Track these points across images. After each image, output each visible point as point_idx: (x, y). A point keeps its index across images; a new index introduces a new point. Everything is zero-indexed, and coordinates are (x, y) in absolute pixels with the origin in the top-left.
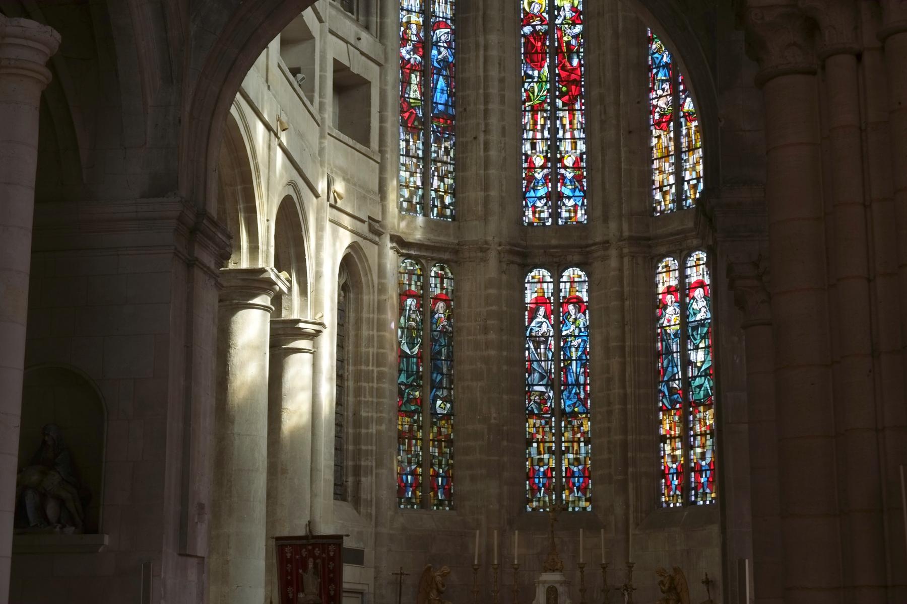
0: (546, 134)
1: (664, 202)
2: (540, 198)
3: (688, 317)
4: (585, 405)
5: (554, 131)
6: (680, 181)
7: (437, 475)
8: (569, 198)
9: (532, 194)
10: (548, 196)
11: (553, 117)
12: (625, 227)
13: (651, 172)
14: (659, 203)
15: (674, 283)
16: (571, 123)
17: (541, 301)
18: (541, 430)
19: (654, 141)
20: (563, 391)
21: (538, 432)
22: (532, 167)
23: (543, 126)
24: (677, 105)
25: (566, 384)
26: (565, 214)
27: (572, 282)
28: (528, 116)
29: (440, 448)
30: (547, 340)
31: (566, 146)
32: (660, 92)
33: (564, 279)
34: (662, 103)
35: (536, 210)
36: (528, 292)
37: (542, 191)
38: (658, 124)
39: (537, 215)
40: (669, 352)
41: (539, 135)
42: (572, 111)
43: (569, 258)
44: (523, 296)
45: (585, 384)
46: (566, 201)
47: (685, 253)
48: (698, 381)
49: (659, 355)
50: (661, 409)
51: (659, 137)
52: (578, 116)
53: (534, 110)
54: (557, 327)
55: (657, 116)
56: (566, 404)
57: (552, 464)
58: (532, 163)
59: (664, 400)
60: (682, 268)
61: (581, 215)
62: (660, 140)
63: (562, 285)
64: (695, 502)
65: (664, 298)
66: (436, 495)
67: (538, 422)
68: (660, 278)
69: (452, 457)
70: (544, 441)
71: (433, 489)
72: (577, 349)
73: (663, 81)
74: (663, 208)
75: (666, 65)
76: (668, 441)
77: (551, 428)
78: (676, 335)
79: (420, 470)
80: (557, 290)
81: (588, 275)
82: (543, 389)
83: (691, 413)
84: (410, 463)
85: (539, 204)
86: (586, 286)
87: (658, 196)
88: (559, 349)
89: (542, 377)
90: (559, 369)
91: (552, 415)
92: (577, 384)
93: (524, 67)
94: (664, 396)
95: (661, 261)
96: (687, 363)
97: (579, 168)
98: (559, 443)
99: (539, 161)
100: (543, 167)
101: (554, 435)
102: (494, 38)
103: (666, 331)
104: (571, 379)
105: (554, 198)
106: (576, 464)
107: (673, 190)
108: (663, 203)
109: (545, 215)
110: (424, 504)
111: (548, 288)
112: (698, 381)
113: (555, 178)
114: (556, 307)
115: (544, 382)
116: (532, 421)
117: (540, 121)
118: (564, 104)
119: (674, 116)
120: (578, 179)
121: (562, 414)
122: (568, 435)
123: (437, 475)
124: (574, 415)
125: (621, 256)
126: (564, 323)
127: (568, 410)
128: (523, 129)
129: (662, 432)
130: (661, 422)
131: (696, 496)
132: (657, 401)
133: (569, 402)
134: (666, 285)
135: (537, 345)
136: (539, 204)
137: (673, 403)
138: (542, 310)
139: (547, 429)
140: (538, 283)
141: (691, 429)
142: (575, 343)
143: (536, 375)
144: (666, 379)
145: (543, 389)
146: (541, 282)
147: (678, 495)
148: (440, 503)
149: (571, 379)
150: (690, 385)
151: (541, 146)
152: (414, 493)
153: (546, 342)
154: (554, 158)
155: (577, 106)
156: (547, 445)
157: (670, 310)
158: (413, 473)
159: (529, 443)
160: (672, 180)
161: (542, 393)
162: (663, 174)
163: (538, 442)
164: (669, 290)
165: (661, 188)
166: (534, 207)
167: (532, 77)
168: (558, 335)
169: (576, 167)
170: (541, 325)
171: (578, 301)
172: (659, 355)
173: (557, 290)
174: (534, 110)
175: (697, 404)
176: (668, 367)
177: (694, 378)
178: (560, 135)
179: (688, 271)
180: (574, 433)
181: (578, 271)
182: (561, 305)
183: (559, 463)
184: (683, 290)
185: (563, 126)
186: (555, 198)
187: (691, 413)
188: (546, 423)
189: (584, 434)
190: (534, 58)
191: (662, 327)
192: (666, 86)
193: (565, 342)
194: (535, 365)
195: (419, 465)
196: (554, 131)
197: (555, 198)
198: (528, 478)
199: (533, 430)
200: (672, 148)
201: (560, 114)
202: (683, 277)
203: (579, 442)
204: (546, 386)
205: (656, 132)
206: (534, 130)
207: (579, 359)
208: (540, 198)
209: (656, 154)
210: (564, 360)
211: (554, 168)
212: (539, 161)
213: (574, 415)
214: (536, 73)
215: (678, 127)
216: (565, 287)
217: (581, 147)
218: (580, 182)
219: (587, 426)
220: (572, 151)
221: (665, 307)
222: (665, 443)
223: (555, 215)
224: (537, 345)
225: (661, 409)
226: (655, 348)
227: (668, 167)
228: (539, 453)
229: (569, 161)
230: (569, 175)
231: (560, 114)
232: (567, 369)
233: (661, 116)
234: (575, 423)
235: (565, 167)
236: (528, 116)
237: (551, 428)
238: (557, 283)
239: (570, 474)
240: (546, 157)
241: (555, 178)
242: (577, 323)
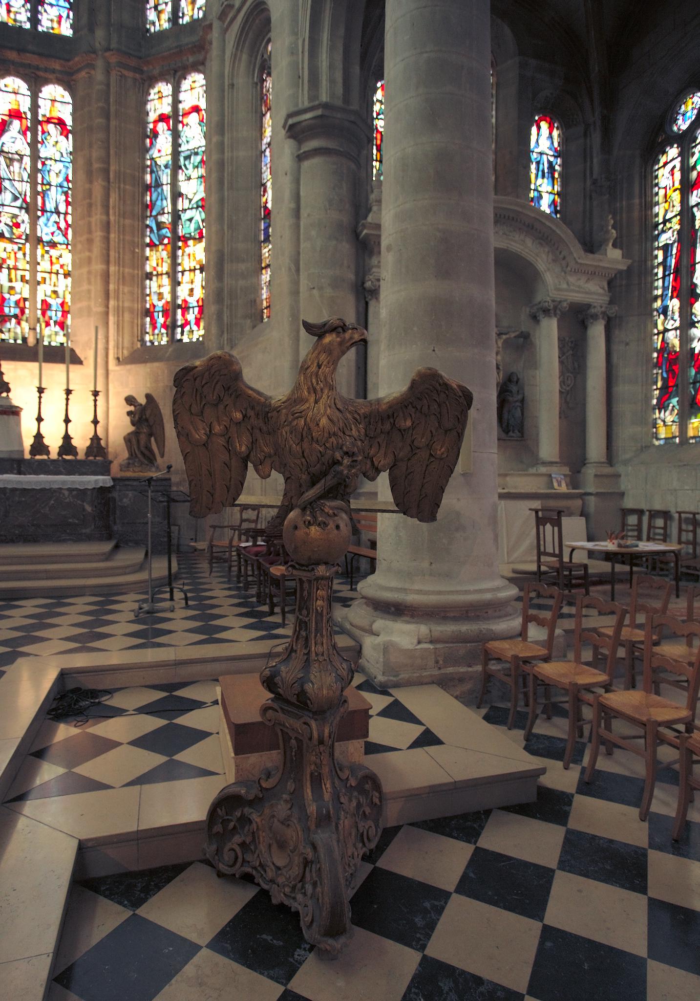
3: (180, 145)
14: (153, 23)
18: (12, 255)
20: (39, 217)
21: (9, 258)
30: (22, 159)
39: (12, 15)
40: (159, 185)
45: (66, 214)
47: (179, 74)
49: (148, 188)
54: (34, 145)
59: (152, 236)
61: (66, 30)
64: (181, 340)
65: (155, 127)
68: (149, 106)
74: (157, 28)
76: (154, 278)
77: (24, 254)
78: (166, 167)
80: (35, 107)
82: (16, 211)
83: (180, 248)
87: (152, 15)
88: (35, 171)
89: (16, 198)
90: (35, 193)
91: (27, 240)
94: (152, 231)
96: (177, 195)
98: (34, 272)
101: (28, 262)
103: (156, 162)
104: (50, 206)
106: (54, 296)
108: (157, 24)
111: (25, 105)
115: (18, 203)
121: (40, 240)
124: (53, 245)
125: (108, 72)
129: (148, 269)
131: (182, 333)
132: (144, 236)
134: (159, 112)
137: (161, 238)
141: (179, 264)
144: (154, 213)
145: (16, 211)
147: (162, 334)
150: (179, 218)
156: (20, 273)
161: (15, 216)
163: (9, 268)
164: (163, 118)
168: (35, 156)
171: (61, 123)
172: (148, 188)
173: (35, 107)
175: (185, 239)
176: (157, 199)
177: (184, 211)
182: (41, 123)
183: (34, 292)
187: (180, 248)
188: (20, 249)
191: (152, 159)
193: (43, 164)
202: (176, 102)
210: (43, 184)
213: (53, 245)
222: (151, 280)
225: (148, 245)
232: (44, 194)
237: (24, 254)
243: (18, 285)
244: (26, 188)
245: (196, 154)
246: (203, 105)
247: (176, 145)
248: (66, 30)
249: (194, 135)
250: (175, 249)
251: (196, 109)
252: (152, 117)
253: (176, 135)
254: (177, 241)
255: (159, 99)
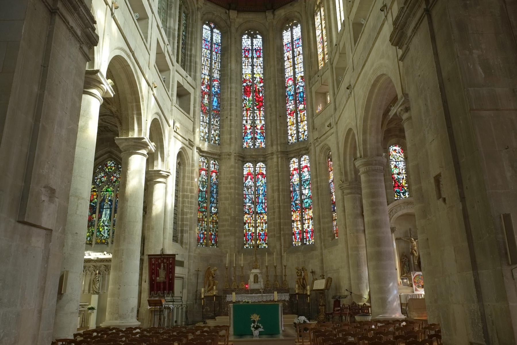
0: (251, 118)
1: (292, 140)
2: (249, 139)
4: (265, 210)
5: (254, 117)
6: (298, 132)
7: (212, 235)
8: (259, 139)
9: (246, 138)
10: (252, 138)
11: (254, 113)
12: (279, 148)
13: (287, 130)
14: (291, 140)
15: (296, 167)
16: (259, 115)
17: (249, 174)
19: (288, 120)
22: (246, 129)
23: (250, 115)
24: (296, 107)
25: (258, 203)
26: (257, 145)
27: (260, 167)
28: (245, 112)
29: (213, 225)
31: (258, 122)
32: (290, 104)
33: (257, 166)
34: (291, 107)
35: (248, 143)
36: (245, 171)
37: (249, 137)
38: (290, 114)
40: (295, 191)
41: (248, 118)
42: (260, 111)
43: (259, 159)
44: (243, 172)
45: (265, 203)
46: (258, 140)
48: (306, 200)
49: (291, 192)
50: (292, 211)
51: (290, 118)
52: (262, 112)
53: (247, 110)
54: (255, 183)
55: (289, 112)
56: (259, 210)
57: (253, 231)
58: (246, 127)
60: (299, 161)
61: (263, 145)
62: (291, 119)
63: (257, 169)
66: (211, 242)
67: (248, 216)
68: (291, 165)
69: (217, 228)
70: (251, 223)
71: (210, 240)
72: (262, 190)
73: (291, 100)
75: (292, 95)
78: (297, 185)
79: (205, 233)
80: (255, 170)
81: (265, 165)
82: (250, 204)
84: (202, 230)
85: (248, 141)
86: (265, 169)
87: (290, 138)
88: (256, 190)
89: (250, 200)
91: (253, 213)
92: (262, 203)
93: (243, 96)
94: (293, 206)
95: (291, 159)
96: (302, 194)
97: (263, 129)
98: (256, 223)
99: (248, 127)
100: (250, 129)
102: (233, 85)
104: (260, 201)
105: (254, 139)
107: (296, 135)
109: (251, 145)
110: (207, 245)
111: (252, 170)
112: (306, 200)
113: (254, 132)
114: (255, 176)
116: (246, 216)
117: (249, 114)
118: (257, 108)
119: (296, 111)
120: (262, 133)
121: (257, 213)
122: (259, 221)
123: (212, 235)
124: (261, 213)
125: (278, 158)
126: (257, 181)
127: (259, 212)
128: (243, 116)
130: (292, 215)
132: (291, 208)
133: (259, 209)
135: (248, 189)
136: (248, 141)
137: (297, 208)
138: (250, 177)
139: (251, 218)
140: (248, 168)
142: (261, 188)
143: (248, 200)
145: (250, 204)
146: (249, 167)
148: (213, 245)
149: (260, 201)
150: (303, 202)
151: (249, 122)
152: (203, 241)
153: (251, 188)
154: (254, 126)
155: (262, 109)
157: (295, 176)
158: (203, 234)
159: (245, 224)
160: (295, 132)
161: (250, 206)
162: (292, 130)
164: (295, 169)
165: (291, 135)
166: (247, 142)
167: (246, 99)
168: (255, 186)
169: (261, 129)
170: (249, 182)
172: (291, 192)
173: (255, 170)
174: (247, 110)
178: (256, 118)
179: (301, 163)
180: (261, 220)
181: (262, 164)
182: (256, 175)
183: (256, 230)
184: (300, 169)
185: (257, 115)
186: (254, 139)
189: (264, 220)
190: (247, 92)
192: (292, 102)
193: (258, 188)
194: (247, 196)
195: (205, 231)
196: (254, 117)
197: (254, 139)
198: (245, 236)
199: (246, 219)
200: (295, 122)
201: (256, 111)
202: (300, 164)
203: (263, 223)
204: (251, 203)
205: (289, 117)
206: (247, 116)
207: (263, 194)
208: (249, 139)
209: (289, 124)
211: (254, 130)
212: (248, 127)
213: (261, 213)
214: (248, 98)
215: (297, 114)
216: (258, 169)
217: (263, 122)
218: (263, 134)
219: (266, 217)
220: (260, 124)
221: (293, 175)
223: (254, 145)
224: (248, 189)
225: (292, 211)
226: (290, 189)
227: (294, 128)
228: (249, 227)
229: (259, 127)
230: (259, 131)
231: (256, 111)
232: (258, 198)
233: (291, 111)
234: (261, 216)
235: (258, 129)
236: (245, 112)
238: (255, 168)
239: (260, 235)
240: (251, 126)
241: (254, 132)
242: (261, 181)
243: (251, 228)
244: (253, 196)
245: (307, 181)
246: (309, 165)
247: (300, 178)
248: (263, 145)
249: (306, 175)
250: (302, 212)
251: (306, 167)
252: (292, 169)
253: (300, 175)
254: (303, 210)
255: (294, 165)
